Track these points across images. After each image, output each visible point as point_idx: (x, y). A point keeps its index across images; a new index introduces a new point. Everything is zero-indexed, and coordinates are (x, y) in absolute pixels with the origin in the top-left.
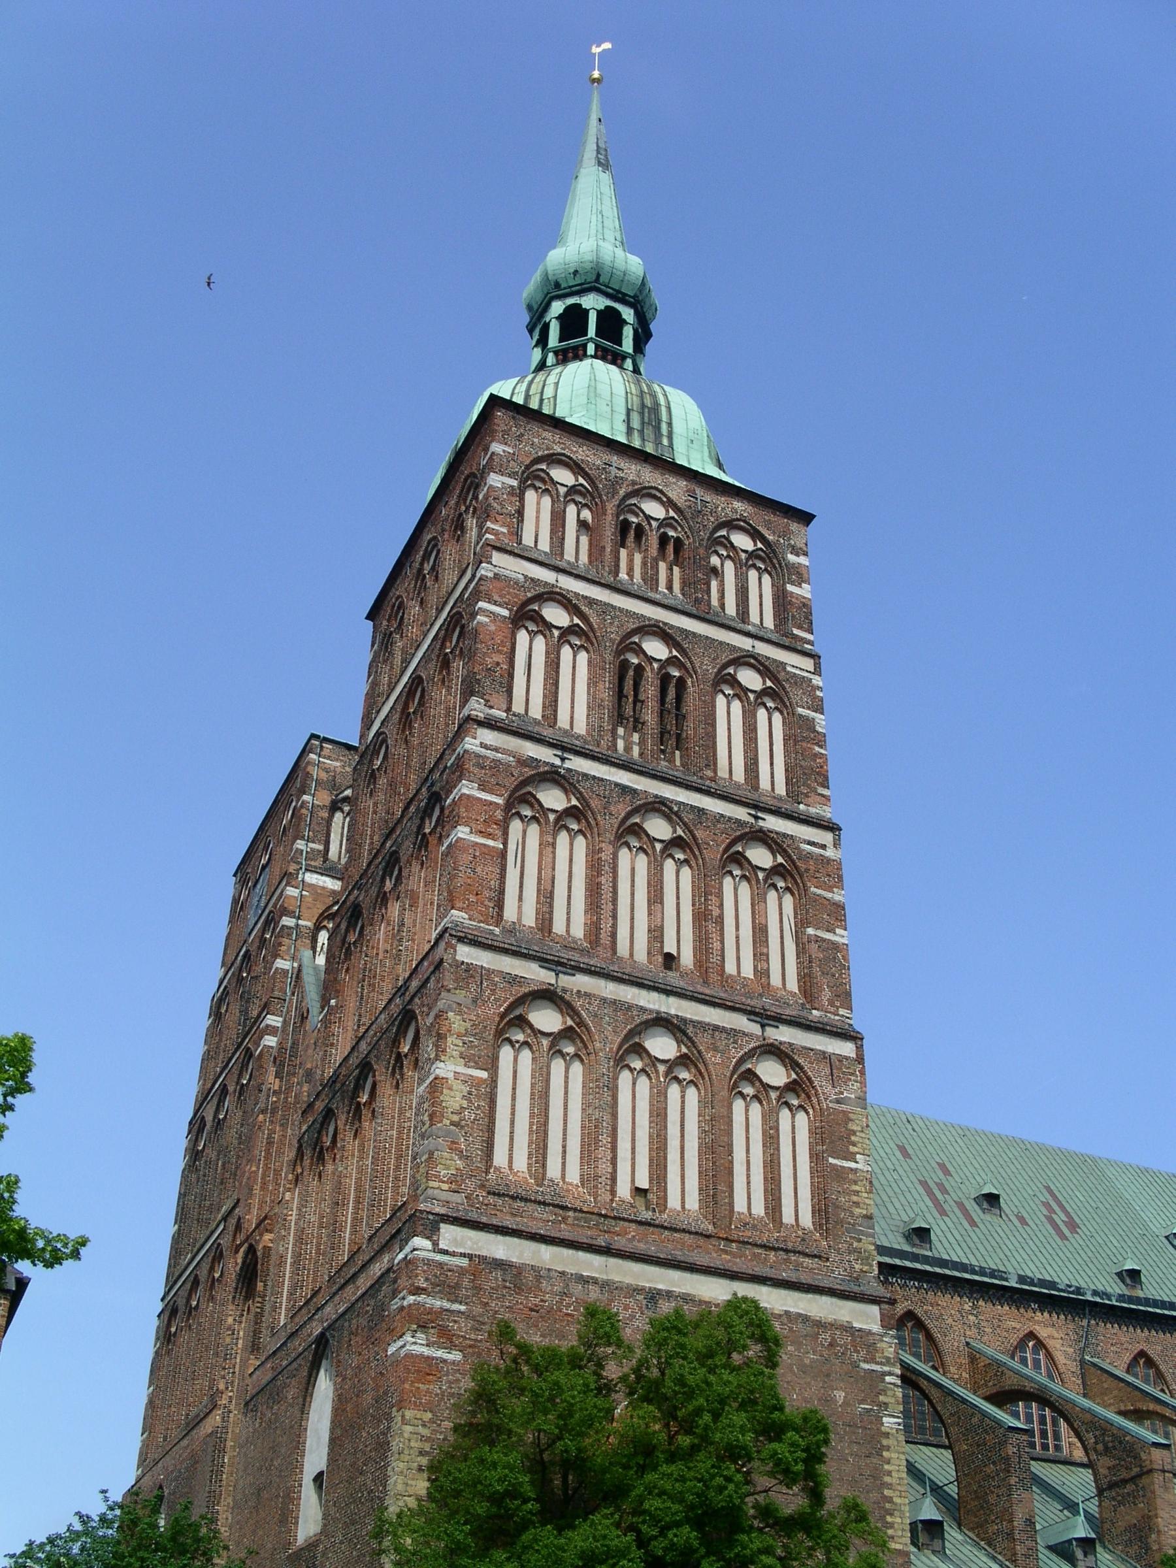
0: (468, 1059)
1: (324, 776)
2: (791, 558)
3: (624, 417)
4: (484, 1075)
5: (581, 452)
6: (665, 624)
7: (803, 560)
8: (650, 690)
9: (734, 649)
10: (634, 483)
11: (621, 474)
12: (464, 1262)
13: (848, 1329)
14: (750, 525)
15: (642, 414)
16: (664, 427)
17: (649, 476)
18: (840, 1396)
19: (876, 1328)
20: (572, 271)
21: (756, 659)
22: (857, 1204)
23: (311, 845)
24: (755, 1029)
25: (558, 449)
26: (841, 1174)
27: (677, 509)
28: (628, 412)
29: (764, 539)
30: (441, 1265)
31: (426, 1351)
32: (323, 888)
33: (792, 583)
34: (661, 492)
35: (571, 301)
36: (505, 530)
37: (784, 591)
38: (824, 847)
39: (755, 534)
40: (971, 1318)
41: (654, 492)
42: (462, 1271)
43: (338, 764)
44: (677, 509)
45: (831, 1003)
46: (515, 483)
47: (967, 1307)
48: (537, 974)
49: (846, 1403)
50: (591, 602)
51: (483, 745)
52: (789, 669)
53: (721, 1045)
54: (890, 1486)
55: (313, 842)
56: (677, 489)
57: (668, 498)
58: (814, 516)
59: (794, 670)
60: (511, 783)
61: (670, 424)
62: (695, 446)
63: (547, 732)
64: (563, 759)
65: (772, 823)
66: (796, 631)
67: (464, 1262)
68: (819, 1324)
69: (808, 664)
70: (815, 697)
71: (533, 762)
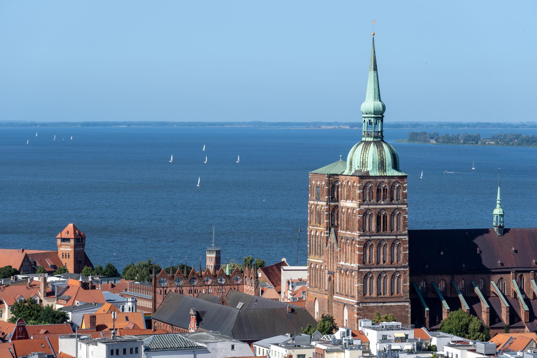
0: (361, 283)
2: (404, 185)
3: (378, 166)
4: (363, 284)
5: (371, 180)
7: (406, 185)
8: (382, 220)
9: (394, 208)
10: (380, 182)
11: (378, 181)
12: (362, 307)
13: (405, 305)
15: (381, 163)
16: (385, 164)
17: (382, 180)
18: (403, 313)
19: (408, 304)
20: (369, 112)
22: (407, 289)
24: (395, 269)
26: (404, 286)
28: (379, 164)
30: (359, 308)
31: (359, 317)
33: (404, 190)
35: (370, 119)
36: (361, 200)
38: (406, 238)
39: (399, 183)
40: (433, 278)
42: (362, 308)
45: (405, 262)
46: (362, 191)
47: (433, 277)
48: (368, 270)
49: (404, 314)
51: (360, 239)
53: (390, 273)
54: (409, 322)
56: (386, 180)
59: (404, 208)
60: (364, 243)
61: (385, 164)
62: (389, 166)
63: (368, 234)
64: (370, 237)
65: (399, 237)
66: (404, 200)
67: (362, 307)
68: (401, 306)
69: (406, 206)
70: (406, 212)
71: (367, 239)
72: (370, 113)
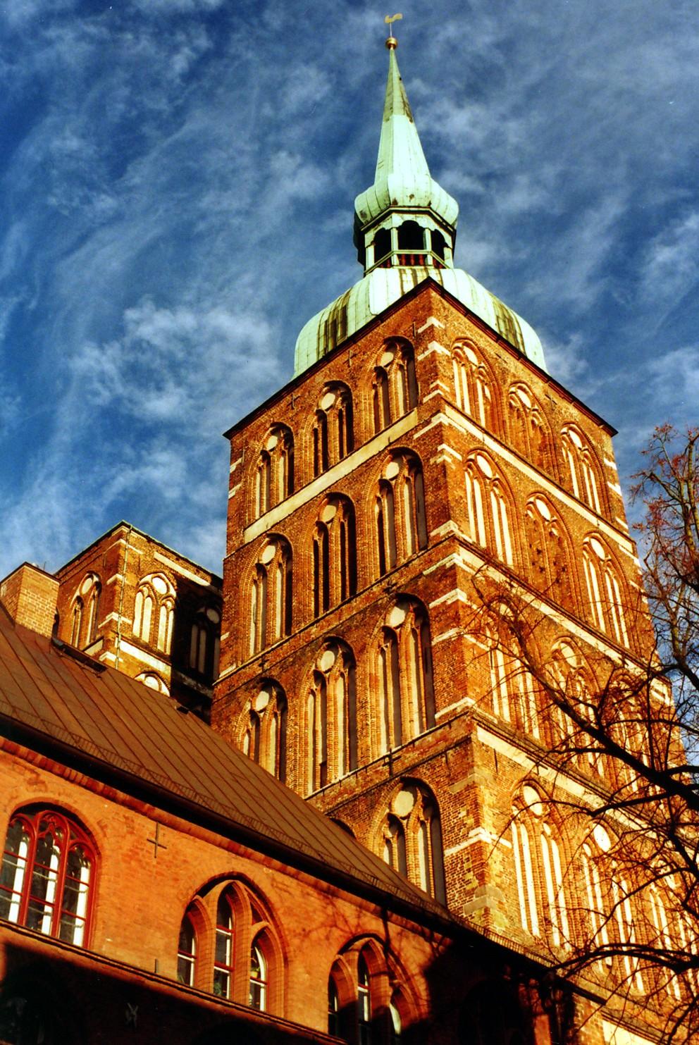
1: (132, 561)
6: (550, 493)
14: (581, 429)
20: (409, 195)
21: (601, 535)
23: (123, 618)
25: (468, 334)
27: (540, 404)
29: (590, 442)
32: (134, 658)
34: (529, 387)
37: (606, 486)
38: (664, 695)
41: (524, 386)
43: (141, 553)
44: (540, 404)
50: (507, 464)
52: (621, 548)
55: (124, 616)
57: (534, 394)
58: (617, 432)
61: (521, 335)
72: (412, 196)
